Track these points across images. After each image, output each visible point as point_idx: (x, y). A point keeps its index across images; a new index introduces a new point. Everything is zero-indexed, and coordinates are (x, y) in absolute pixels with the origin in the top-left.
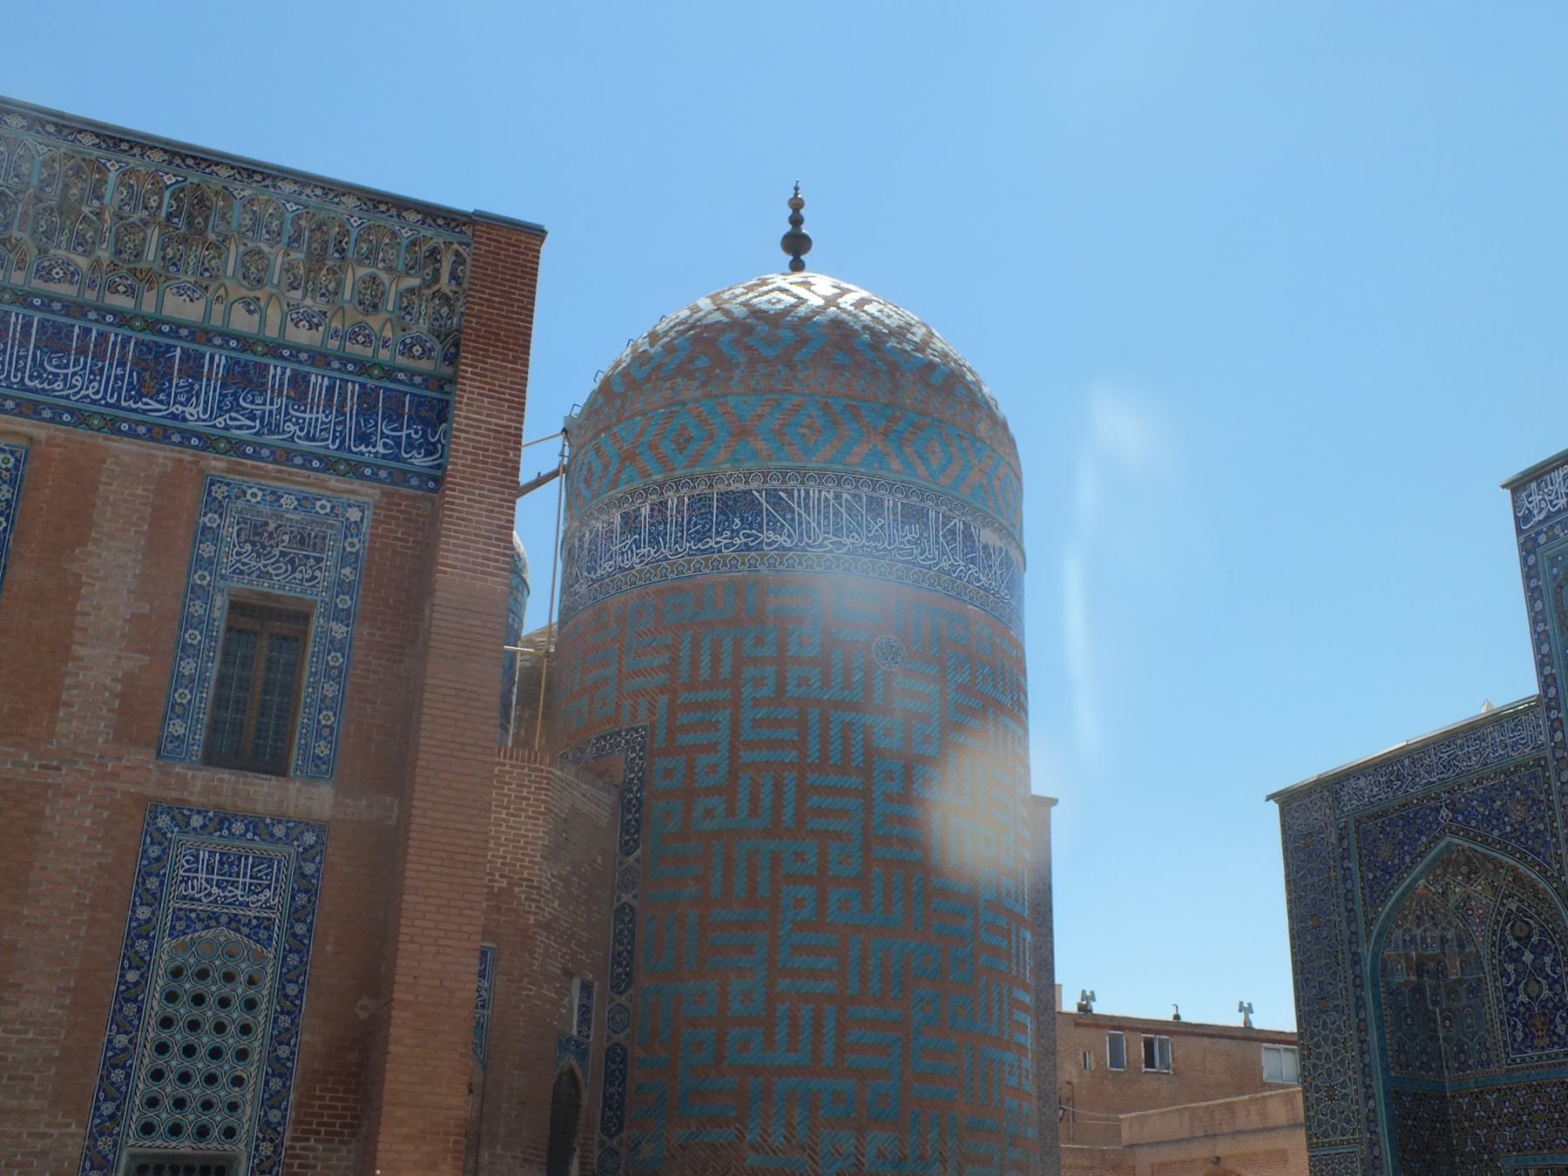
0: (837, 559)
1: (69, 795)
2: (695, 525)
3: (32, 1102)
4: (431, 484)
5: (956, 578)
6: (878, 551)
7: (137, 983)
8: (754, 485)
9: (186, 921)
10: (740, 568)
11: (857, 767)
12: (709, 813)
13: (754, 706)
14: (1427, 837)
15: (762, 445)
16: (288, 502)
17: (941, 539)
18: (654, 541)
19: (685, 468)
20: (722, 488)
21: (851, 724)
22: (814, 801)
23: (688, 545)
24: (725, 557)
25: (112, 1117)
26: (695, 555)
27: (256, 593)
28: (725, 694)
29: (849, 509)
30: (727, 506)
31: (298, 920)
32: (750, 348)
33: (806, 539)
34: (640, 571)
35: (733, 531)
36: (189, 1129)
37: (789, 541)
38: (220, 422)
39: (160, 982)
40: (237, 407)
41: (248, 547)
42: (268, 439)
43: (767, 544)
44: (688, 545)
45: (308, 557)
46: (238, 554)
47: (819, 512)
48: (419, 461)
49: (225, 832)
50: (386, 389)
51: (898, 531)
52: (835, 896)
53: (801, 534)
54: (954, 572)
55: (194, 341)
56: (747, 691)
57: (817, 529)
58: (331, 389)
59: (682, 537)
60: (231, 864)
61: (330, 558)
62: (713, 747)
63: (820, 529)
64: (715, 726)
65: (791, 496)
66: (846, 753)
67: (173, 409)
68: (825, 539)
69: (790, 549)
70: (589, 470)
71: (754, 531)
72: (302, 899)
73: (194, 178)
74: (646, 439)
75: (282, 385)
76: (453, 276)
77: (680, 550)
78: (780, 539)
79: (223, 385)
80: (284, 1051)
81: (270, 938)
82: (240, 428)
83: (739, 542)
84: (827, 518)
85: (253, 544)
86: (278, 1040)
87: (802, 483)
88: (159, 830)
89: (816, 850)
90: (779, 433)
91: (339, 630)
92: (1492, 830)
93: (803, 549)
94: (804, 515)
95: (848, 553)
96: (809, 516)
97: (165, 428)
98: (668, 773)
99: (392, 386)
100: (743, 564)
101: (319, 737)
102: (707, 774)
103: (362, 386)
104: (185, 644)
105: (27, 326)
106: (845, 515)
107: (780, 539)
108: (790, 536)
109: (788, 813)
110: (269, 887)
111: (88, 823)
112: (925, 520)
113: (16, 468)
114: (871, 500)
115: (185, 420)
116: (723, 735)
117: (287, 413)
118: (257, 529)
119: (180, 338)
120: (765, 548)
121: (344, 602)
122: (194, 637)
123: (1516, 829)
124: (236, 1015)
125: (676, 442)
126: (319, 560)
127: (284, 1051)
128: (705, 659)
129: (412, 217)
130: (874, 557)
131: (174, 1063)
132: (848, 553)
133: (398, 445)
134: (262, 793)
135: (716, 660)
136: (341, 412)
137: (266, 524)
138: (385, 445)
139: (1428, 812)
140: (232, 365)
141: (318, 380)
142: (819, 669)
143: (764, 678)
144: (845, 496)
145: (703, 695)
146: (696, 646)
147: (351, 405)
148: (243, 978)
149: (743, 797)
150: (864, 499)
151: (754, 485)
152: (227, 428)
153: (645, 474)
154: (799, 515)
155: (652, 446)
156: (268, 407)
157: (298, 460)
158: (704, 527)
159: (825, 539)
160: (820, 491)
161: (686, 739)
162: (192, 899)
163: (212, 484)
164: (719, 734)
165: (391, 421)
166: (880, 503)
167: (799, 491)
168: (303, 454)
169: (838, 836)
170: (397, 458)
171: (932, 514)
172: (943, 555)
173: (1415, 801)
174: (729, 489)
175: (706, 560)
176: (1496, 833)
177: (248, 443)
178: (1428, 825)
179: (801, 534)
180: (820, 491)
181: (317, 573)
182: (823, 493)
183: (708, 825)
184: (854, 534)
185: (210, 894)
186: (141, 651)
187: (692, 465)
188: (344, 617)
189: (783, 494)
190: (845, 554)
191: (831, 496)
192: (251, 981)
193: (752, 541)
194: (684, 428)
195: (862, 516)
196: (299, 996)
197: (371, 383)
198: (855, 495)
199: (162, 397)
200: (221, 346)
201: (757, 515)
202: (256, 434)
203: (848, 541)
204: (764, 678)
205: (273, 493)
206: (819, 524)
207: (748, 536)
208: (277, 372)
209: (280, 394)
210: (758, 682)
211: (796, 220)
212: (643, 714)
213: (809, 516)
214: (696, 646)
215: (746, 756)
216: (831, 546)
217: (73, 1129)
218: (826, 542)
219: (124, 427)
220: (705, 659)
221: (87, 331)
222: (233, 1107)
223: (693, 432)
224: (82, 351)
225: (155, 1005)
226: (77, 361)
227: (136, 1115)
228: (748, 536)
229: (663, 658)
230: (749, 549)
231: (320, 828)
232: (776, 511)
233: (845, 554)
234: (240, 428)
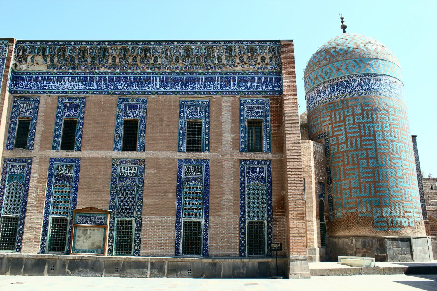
0: (362, 92)
1: (226, 160)
3: (230, 213)
4: (280, 93)
7: (243, 192)
8: (343, 80)
9: (250, 180)
11: (372, 135)
12: (343, 148)
13: (349, 125)
15: (343, 71)
16: (255, 102)
18: (324, 94)
19: (328, 79)
20: (336, 81)
21: (370, 126)
22: (364, 143)
24: (339, 96)
25: (243, 215)
27: (252, 119)
28: (343, 123)
31: (269, 178)
32: (338, 52)
34: (322, 101)
36: (256, 216)
38: (240, 89)
39: (247, 191)
40: (243, 86)
41: (249, 111)
42: (249, 90)
45: (260, 111)
46: (248, 113)
48: (277, 89)
49: (254, 164)
50: (269, 77)
52: (371, 161)
53: (354, 88)
55: (234, 75)
56: (347, 122)
58: (259, 79)
60: (255, 169)
61: (264, 110)
62: (342, 134)
64: (341, 130)
65: (351, 81)
66: (370, 132)
67: (232, 88)
69: (352, 92)
70: (309, 82)
72: (269, 174)
73: (229, 45)
74: (319, 74)
75: (250, 80)
76: (278, 53)
78: (350, 90)
79: (240, 82)
80: (270, 202)
81: (264, 182)
82: (244, 89)
84: (359, 84)
85: (250, 110)
86: (268, 200)
87: (353, 78)
88: (242, 165)
90: (346, 68)
91: (268, 124)
95: (365, 91)
97: (231, 92)
98: (333, 141)
99: (270, 76)
101: (267, 144)
102: (341, 140)
103: (265, 77)
104: (241, 131)
105: (206, 78)
107: (350, 90)
108: (352, 89)
109: (359, 146)
110: (263, 173)
111: (230, 165)
113: (208, 104)
114: (368, 79)
115: (234, 90)
116: (343, 132)
117: (252, 85)
118: (250, 107)
119: (231, 75)
121: (268, 118)
122: (242, 129)
124: (260, 196)
125: (325, 74)
126: (262, 111)
127: (270, 202)
128: (338, 117)
129: (268, 43)
131: (251, 205)
132: (365, 91)
133: (273, 87)
134: (259, 156)
135: (340, 117)
136: (262, 83)
137: (252, 106)
138: (271, 87)
140: (241, 77)
141: (256, 78)
144: (362, 79)
145: (338, 124)
146: (335, 114)
147: (263, 80)
148: (261, 189)
149: (349, 144)
151: (343, 80)
152: (242, 90)
153: (320, 81)
155: (320, 75)
156: (248, 85)
157: (255, 93)
161: (335, 134)
162: (250, 176)
163: (241, 100)
165: (271, 83)
166: (370, 79)
168: (256, 92)
169: (370, 149)
170: (273, 90)
177: (246, 92)
179: (354, 88)
181: (262, 114)
182: (358, 79)
183: (343, 150)
185: (252, 175)
186: (234, 133)
187: (329, 78)
188: (268, 121)
189: (349, 81)
191: (359, 80)
192: (262, 190)
194: (326, 71)
196: (271, 192)
197: (266, 76)
199: (230, 86)
200: (238, 75)
202: (247, 90)
203: (364, 88)
204: (350, 119)
205: (252, 100)
207: (343, 91)
208: (249, 77)
209: (250, 82)
210: (349, 120)
211: (343, 22)
212: (327, 130)
214: (335, 114)
215: (349, 135)
217: (237, 217)
219: (224, 93)
220: (338, 117)
221: (215, 77)
222: (262, 212)
223: (328, 71)
224: (215, 81)
225: (247, 195)
226: (215, 83)
227: (247, 215)
228: (343, 91)
229: (329, 118)
230: (343, 93)
231: (270, 161)
234: (244, 89)
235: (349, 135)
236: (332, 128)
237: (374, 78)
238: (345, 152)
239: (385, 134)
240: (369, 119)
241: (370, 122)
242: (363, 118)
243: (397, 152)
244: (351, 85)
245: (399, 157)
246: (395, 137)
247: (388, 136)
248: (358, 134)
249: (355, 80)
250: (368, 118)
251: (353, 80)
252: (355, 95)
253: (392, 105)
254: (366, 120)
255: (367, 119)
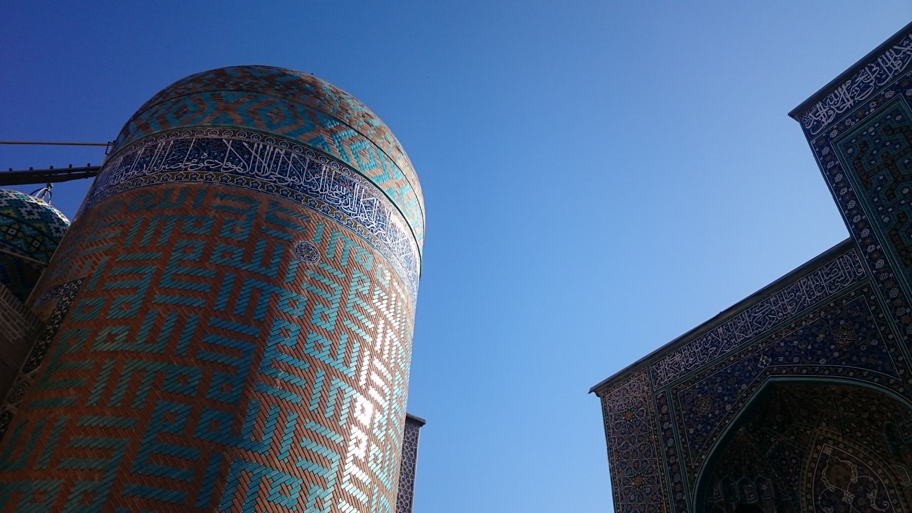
0: (278, 187)
2: (173, 155)
5: (369, 229)
6: (313, 192)
8: (226, 136)
10: (198, 180)
12: (111, 338)
14: (747, 384)
17: (361, 202)
21: (260, 290)
22: (211, 338)
23: (163, 166)
26: (167, 172)
29: (294, 163)
30: (201, 145)
33: (256, 171)
35: (200, 159)
37: (242, 170)
43: (224, 169)
44: (163, 166)
47: (271, 159)
51: (329, 185)
53: (253, 168)
54: (368, 225)
56: (176, 255)
57: (266, 168)
59: (160, 163)
63: (269, 168)
65: (252, 146)
68: (271, 174)
71: (216, 161)
77: (156, 170)
83: (202, 165)
84: (276, 163)
87: (262, 141)
89: (200, 376)
92: (818, 360)
93: (253, 176)
94: (258, 158)
96: (263, 159)
100: (202, 177)
106: (290, 165)
108: (244, 167)
112: (351, 188)
120: (222, 170)
123: (844, 353)
130: (307, 193)
139: (746, 363)
142: (244, 249)
143: (194, 247)
144: (293, 155)
150: (308, 161)
154: (255, 157)
158: (180, 156)
159: (271, 174)
160: (275, 148)
164: (142, 282)
166: (320, 167)
167: (258, 145)
171: (357, 187)
172: (361, 212)
173: (732, 359)
174: (206, 137)
175: (173, 175)
176: (823, 362)
178: (748, 374)
179: (253, 168)
180: (275, 148)
182: (277, 150)
184: (295, 177)
189: (245, 144)
190: (285, 186)
193: (212, 166)
195: (304, 169)
198: (301, 157)
201: (222, 152)
206: (269, 166)
207: (211, 163)
213: (263, 159)
216: (275, 179)
218: (271, 176)
228: (211, 163)
232: (238, 153)
233: (285, 186)
235: (158, 298)
236: (109, 265)
237: (335, 170)
238: (112, 354)
239: (312, 336)
240: (268, 267)
241: (268, 279)
242: (247, 258)
243: (337, 416)
244: (246, 157)
245: (338, 439)
246: (346, 363)
247: (319, 347)
248: (200, 302)
249: (270, 149)
250: (265, 263)
251: (261, 146)
252: (248, 184)
253: (368, 266)
254: (254, 266)
255: (261, 266)
